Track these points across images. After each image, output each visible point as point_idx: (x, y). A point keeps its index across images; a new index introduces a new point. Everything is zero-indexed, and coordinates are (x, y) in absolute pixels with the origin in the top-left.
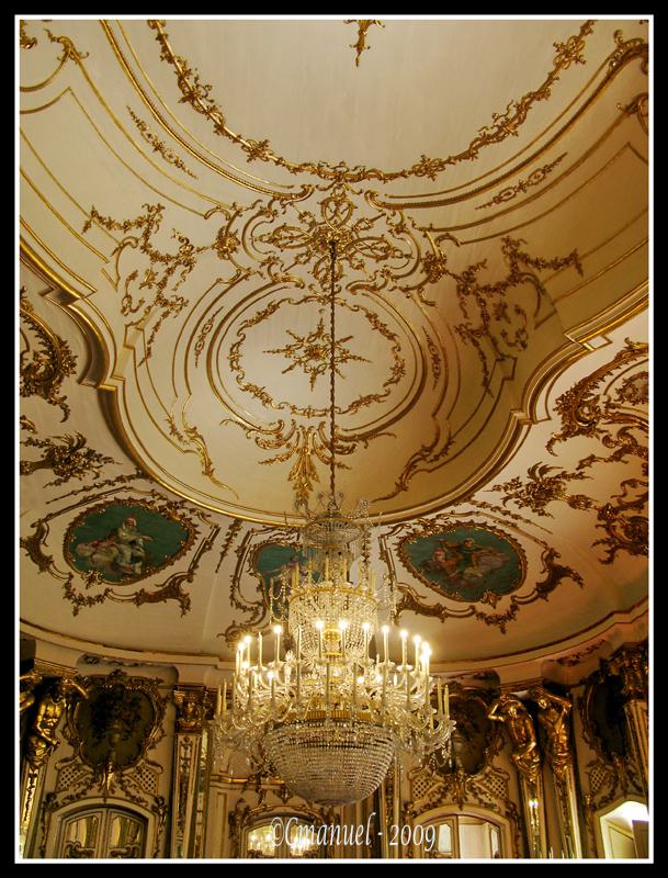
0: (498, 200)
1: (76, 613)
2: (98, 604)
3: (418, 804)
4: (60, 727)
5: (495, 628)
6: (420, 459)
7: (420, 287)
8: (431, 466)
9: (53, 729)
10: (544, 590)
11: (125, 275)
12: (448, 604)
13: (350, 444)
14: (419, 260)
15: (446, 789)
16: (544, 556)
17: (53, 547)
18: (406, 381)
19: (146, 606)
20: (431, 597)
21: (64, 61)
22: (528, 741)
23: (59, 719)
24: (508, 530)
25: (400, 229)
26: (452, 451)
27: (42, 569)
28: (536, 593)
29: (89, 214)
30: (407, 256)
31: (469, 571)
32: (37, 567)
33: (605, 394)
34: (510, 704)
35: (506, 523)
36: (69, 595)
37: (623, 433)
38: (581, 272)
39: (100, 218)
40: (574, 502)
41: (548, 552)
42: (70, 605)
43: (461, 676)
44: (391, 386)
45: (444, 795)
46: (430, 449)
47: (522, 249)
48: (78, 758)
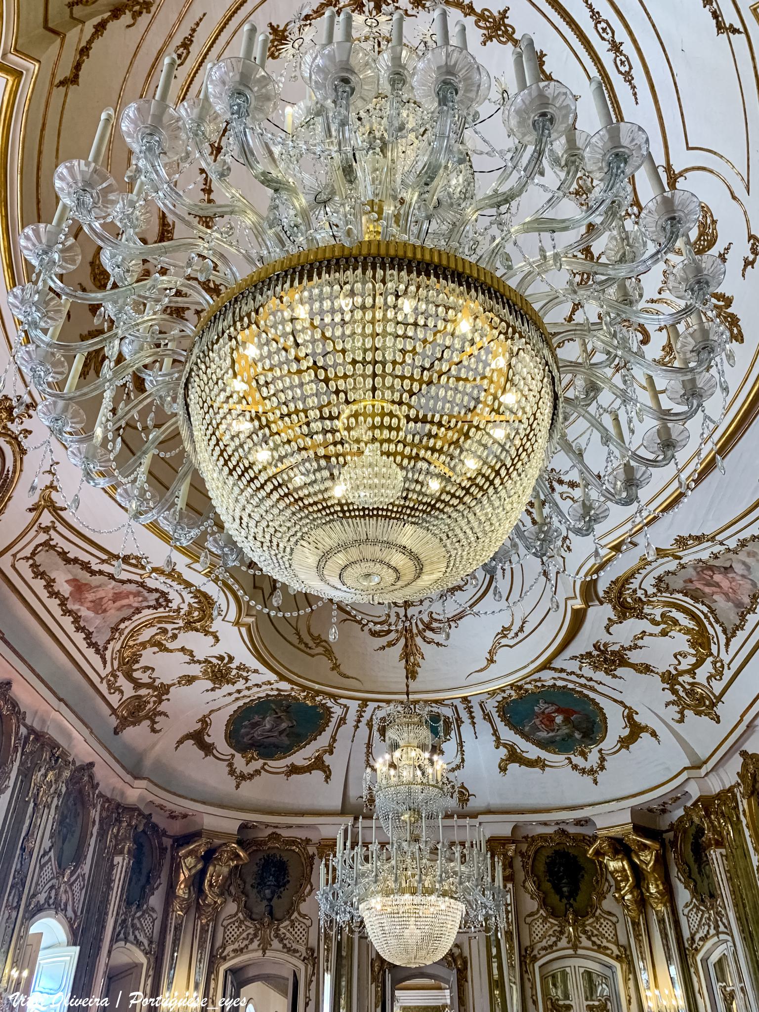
1: (237, 787)
2: (257, 778)
6: (502, 637)
8: (512, 643)
16: (625, 714)
17: (217, 735)
19: (294, 776)
24: (586, 692)
26: (528, 629)
27: (206, 755)
28: (619, 745)
32: (202, 754)
35: (585, 686)
36: (232, 772)
41: (627, 711)
42: (232, 781)
46: (509, 629)
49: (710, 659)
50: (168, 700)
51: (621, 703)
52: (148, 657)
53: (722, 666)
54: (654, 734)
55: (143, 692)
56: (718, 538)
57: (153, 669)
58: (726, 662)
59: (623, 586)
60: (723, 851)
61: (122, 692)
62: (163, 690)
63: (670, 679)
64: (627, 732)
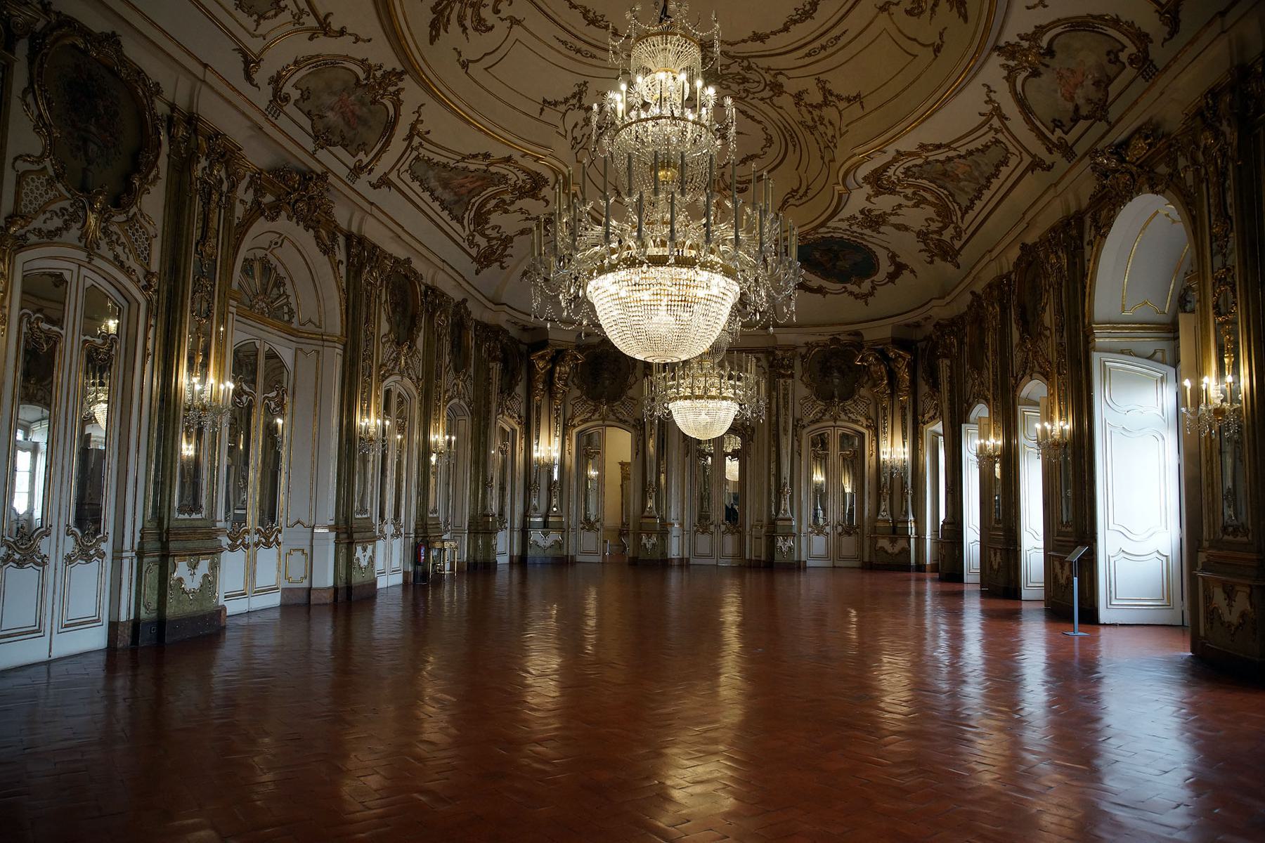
0: (809, 55)
3: (805, 422)
4: (570, 378)
5: (861, 302)
7: (770, 98)
9: (565, 381)
10: (892, 277)
11: (569, 128)
12: (825, 283)
13: (744, 186)
14: (766, 85)
15: (826, 410)
18: (776, 147)
20: (815, 281)
21: (511, 27)
22: (882, 380)
23: (569, 374)
25: (749, 68)
29: (541, 102)
30: (757, 82)
31: (839, 263)
33: (894, 174)
34: (870, 355)
37: (914, 193)
38: (863, 107)
39: (549, 103)
40: (898, 227)
43: (839, 334)
44: (767, 149)
45: (824, 415)
47: (828, 86)
48: (584, 397)
49: (952, 225)
50: (512, 247)
51: (887, 248)
52: (495, 219)
53: (961, 232)
54: (912, 271)
55: (494, 242)
56: (954, 146)
57: (500, 227)
58: (964, 227)
59: (881, 174)
60: (947, 362)
61: (479, 246)
62: (507, 241)
63: (923, 236)
64: (892, 269)
